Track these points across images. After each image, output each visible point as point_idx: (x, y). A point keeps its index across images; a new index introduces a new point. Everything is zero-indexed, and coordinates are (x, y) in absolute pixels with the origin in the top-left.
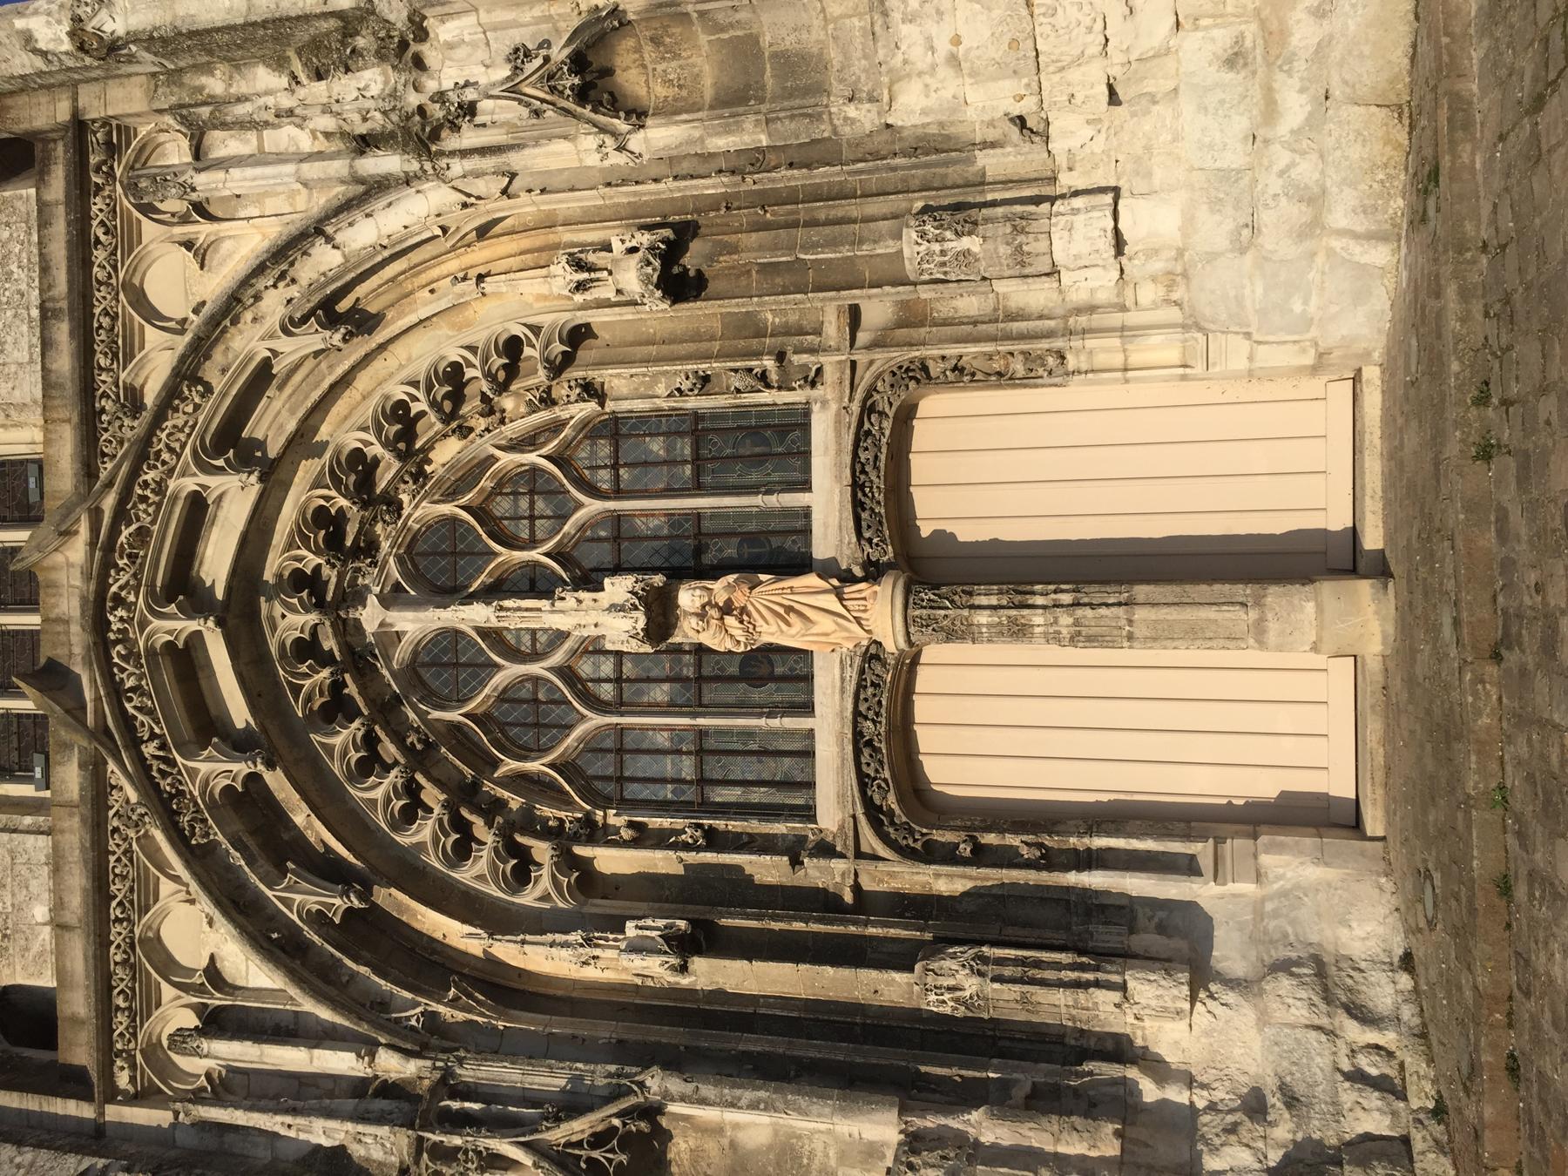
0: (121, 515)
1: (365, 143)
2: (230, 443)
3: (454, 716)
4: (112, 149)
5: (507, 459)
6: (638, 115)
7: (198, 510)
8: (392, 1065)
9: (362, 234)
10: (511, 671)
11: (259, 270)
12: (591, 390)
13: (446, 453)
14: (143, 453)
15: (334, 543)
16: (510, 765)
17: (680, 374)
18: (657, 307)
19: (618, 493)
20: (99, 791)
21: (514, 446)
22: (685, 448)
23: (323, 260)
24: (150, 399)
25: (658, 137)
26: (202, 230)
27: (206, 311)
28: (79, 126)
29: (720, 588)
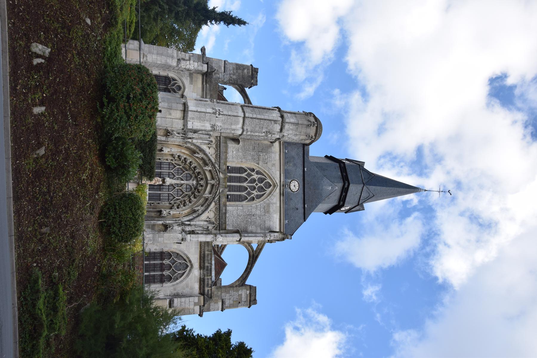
0: (216, 192)
1: (189, 225)
2: (207, 199)
3: (187, 172)
4: (217, 228)
5: (180, 198)
6: (163, 224)
7: (210, 193)
8: (190, 140)
9: (191, 217)
10: (180, 176)
11: (201, 214)
12: (170, 204)
13: (186, 198)
14: (214, 198)
15: (198, 190)
16: (181, 167)
17: (161, 204)
18: (162, 210)
19: (169, 194)
20: (219, 166)
21: (179, 199)
22: (161, 197)
23: (194, 216)
24: (213, 204)
25: (161, 222)
26: (208, 219)
27: (207, 212)
28: (219, 230)
29: (157, 183)
